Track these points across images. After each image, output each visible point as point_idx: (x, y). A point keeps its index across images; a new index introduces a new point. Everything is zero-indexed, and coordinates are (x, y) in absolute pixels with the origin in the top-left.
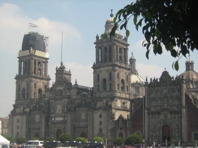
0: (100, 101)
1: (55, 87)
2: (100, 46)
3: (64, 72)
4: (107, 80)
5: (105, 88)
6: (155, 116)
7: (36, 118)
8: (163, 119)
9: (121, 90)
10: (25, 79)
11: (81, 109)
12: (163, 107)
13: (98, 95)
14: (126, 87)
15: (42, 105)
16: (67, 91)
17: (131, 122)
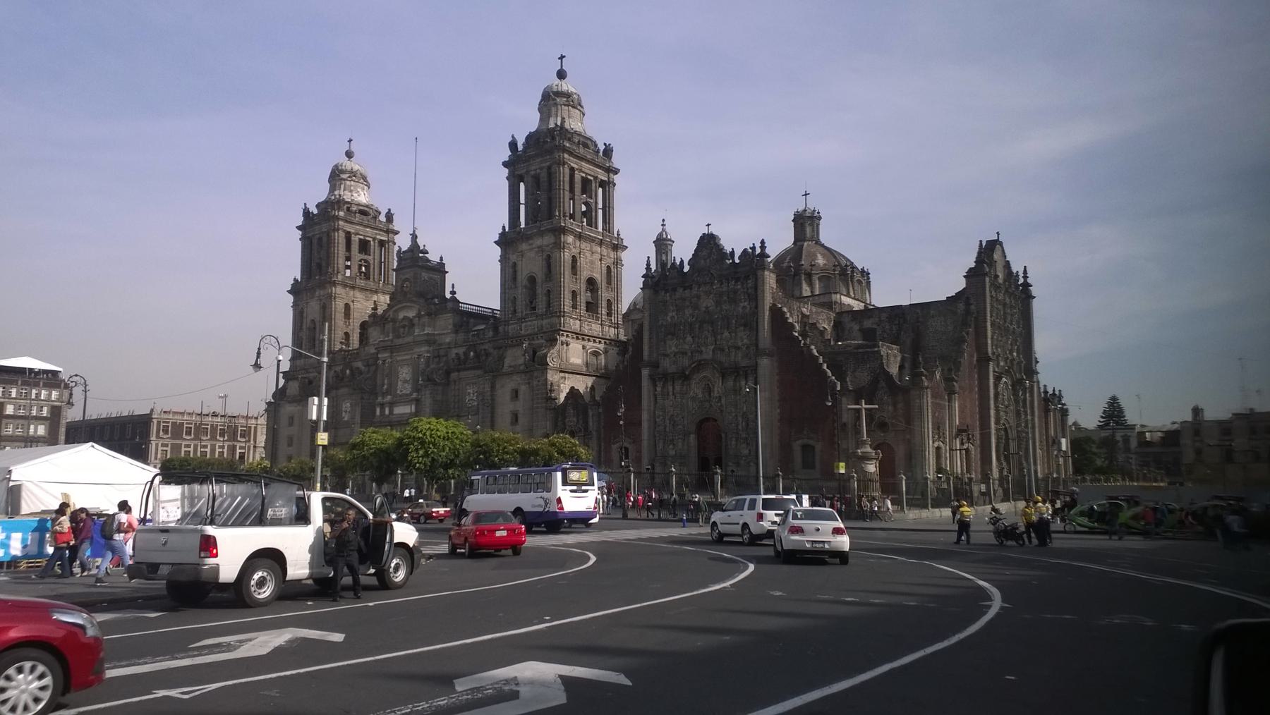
0: (514, 346)
1: (394, 309)
2: (519, 173)
3: (420, 264)
4: (539, 280)
5: (533, 306)
6: (674, 388)
7: (343, 409)
8: (700, 396)
9: (583, 312)
10: (317, 293)
11: (463, 374)
12: (697, 357)
13: (512, 329)
14: (604, 304)
15: (358, 368)
16: (426, 319)
17: (600, 410)
